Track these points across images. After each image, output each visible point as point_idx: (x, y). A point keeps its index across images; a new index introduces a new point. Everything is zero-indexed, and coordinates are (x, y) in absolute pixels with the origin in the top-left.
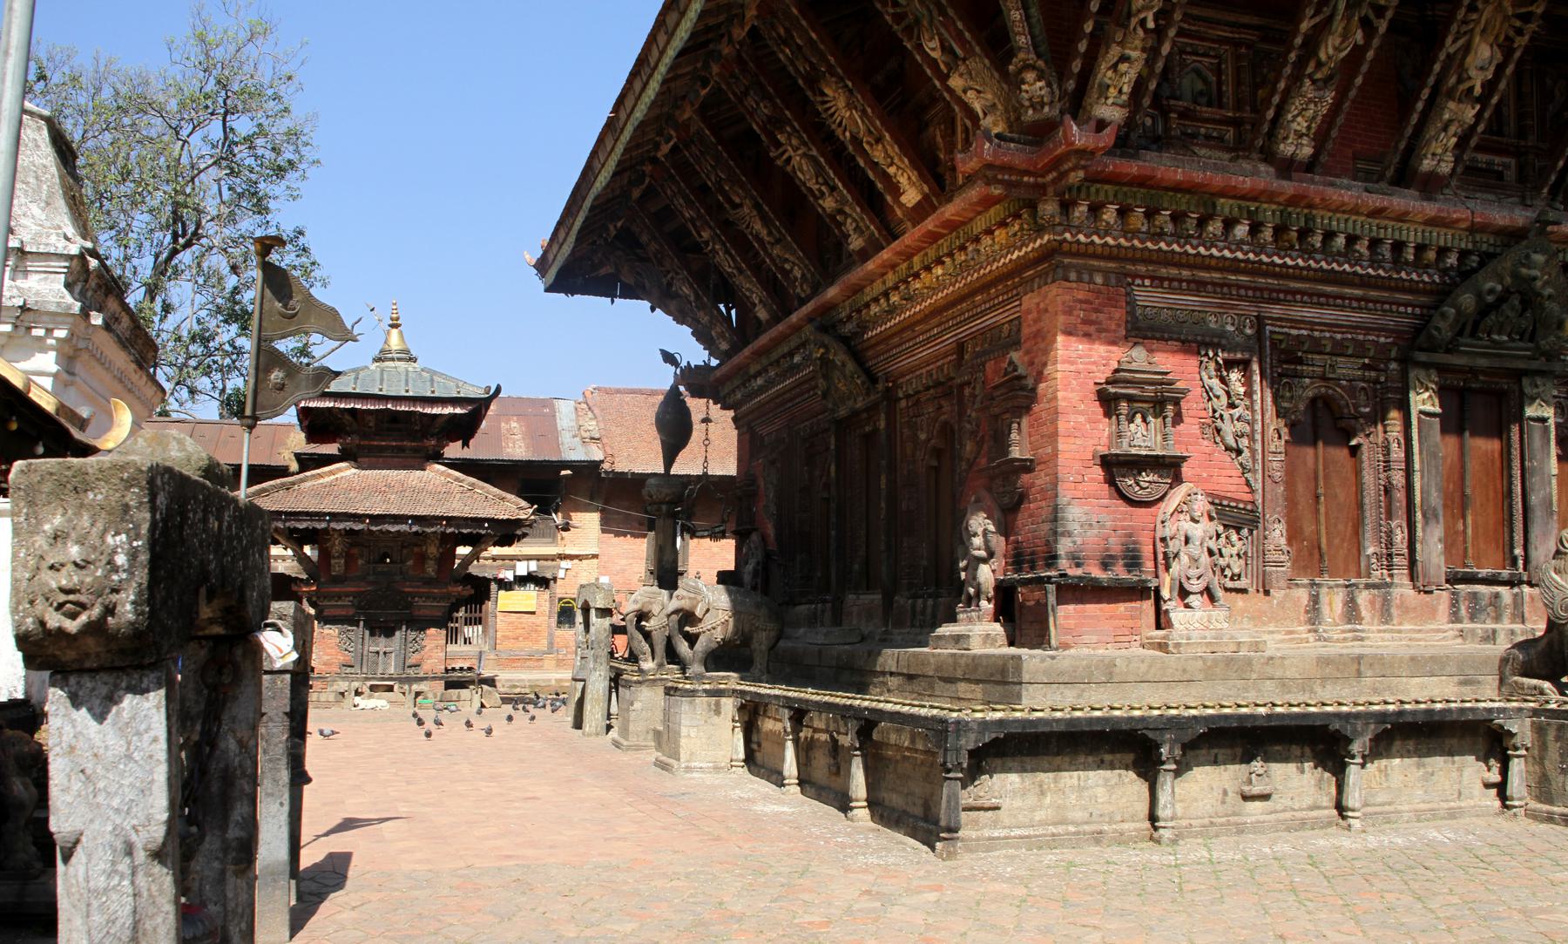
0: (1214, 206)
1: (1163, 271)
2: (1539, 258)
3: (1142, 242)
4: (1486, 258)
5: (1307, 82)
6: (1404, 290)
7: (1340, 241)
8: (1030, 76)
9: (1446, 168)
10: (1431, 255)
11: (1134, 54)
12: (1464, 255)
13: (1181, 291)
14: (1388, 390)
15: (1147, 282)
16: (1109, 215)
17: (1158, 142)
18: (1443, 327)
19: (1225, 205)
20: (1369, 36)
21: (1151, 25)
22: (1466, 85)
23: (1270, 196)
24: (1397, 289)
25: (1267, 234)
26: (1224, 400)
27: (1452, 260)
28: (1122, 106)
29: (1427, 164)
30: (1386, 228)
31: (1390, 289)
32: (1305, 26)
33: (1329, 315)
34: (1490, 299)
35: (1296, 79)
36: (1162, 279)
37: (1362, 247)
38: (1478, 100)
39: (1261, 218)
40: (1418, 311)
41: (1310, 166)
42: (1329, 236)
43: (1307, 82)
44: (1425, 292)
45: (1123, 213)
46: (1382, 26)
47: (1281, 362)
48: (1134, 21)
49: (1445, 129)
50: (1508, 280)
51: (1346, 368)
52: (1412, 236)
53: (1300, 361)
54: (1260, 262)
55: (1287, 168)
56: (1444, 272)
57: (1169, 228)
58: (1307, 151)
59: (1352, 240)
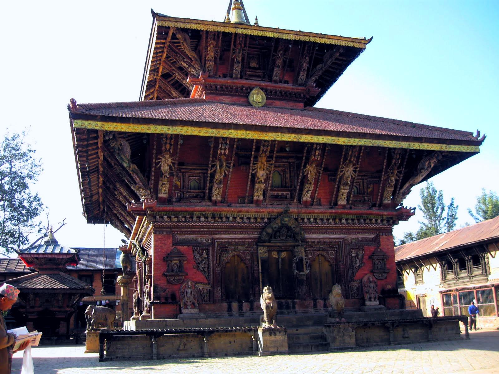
0: (193, 214)
2: (286, 219)
3: (176, 223)
4: (275, 219)
5: (215, 184)
6: (254, 229)
7: (231, 219)
8: (141, 190)
9: (261, 198)
11: (165, 183)
12: (268, 219)
14: (254, 252)
15: (178, 233)
16: (166, 218)
17: (180, 200)
18: (264, 236)
19: (196, 214)
20: (229, 172)
21: (168, 176)
22: (259, 180)
23: (209, 211)
24: (252, 229)
25: (210, 219)
26: (200, 259)
27: (266, 220)
28: (166, 193)
30: (243, 215)
31: (249, 229)
32: (209, 172)
33: (232, 236)
34: (275, 229)
35: (212, 182)
36: (183, 232)
37: (238, 220)
38: (264, 183)
39: (207, 216)
40: (259, 233)
41: (222, 202)
42: (228, 218)
43: (215, 184)
44: (260, 229)
46: (231, 170)
47: (221, 248)
48: (163, 176)
49: (258, 190)
50: (280, 224)
51: (240, 248)
52: (252, 215)
54: (210, 225)
55: (215, 203)
56: (266, 223)
57: (183, 219)
59: (235, 218)
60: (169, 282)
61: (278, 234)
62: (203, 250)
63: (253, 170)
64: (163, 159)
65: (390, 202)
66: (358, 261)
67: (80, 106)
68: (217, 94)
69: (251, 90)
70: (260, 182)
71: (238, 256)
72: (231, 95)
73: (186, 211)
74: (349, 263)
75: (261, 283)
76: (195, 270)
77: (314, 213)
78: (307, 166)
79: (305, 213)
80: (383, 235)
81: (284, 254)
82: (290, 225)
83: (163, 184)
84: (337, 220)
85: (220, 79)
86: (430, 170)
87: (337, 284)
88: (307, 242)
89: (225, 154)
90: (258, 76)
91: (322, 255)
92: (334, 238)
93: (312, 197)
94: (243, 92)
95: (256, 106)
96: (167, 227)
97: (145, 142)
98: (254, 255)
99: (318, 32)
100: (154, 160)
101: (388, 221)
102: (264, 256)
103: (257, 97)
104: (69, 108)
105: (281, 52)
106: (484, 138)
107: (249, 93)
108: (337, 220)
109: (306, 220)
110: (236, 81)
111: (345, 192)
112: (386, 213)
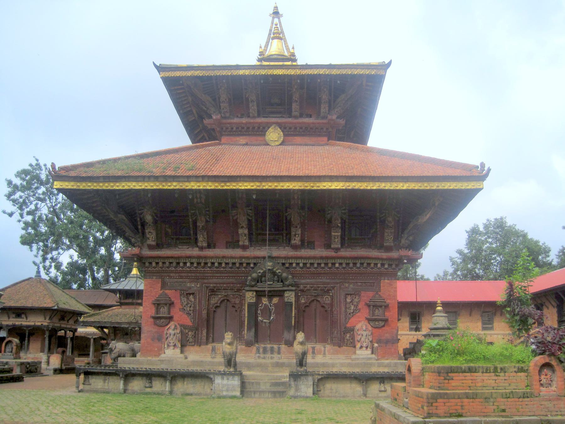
1: (172, 275)
6: (242, 273)
7: (216, 264)
9: (247, 243)
10: (245, 265)
11: (152, 231)
13: (176, 278)
25: (195, 265)
27: (252, 265)
32: (190, 220)
34: (260, 274)
37: (223, 265)
42: (213, 264)
45: (157, 263)
53: (216, 292)
58: (205, 244)
59: (220, 264)
60: (155, 324)
61: (263, 279)
62: (190, 294)
65: (392, 244)
66: (352, 307)
67: (61, 169)
68: (235, 135)
69: (269, 128)
70: (242, 227)
71: (228, 300)
72: (249, 135)
73: (172, 257)
74: (343, 309)
75: (246, 328)
76: (181, 313)
77: (301, 258)
78: (288, 210)
79: (292, 258)
80: (384, 280)
81: (275, 300)
82: (275, 269)
83: (150, 232)
84: (330, 265)
85: (236, 120)
87: (301, 332)
88: (298, 287)
89: (201, 202)
90: (280, 113)
91: (317, 300)
92: (328, 283)
93: (302, 241)
94: (262, 131)
95: (273, 145)
96: (158, 272)
98: (243, 298)
99: (327, 63)
101: (390, 265)
102: (251, 301)
103: (274, 135)
105: (296, 87)
106: (489, 170)
107: (266, 131)
108: (330, 265)
109: (294, 265)
110: (252, 121)
111: (338, 236)
112: (384, 255)
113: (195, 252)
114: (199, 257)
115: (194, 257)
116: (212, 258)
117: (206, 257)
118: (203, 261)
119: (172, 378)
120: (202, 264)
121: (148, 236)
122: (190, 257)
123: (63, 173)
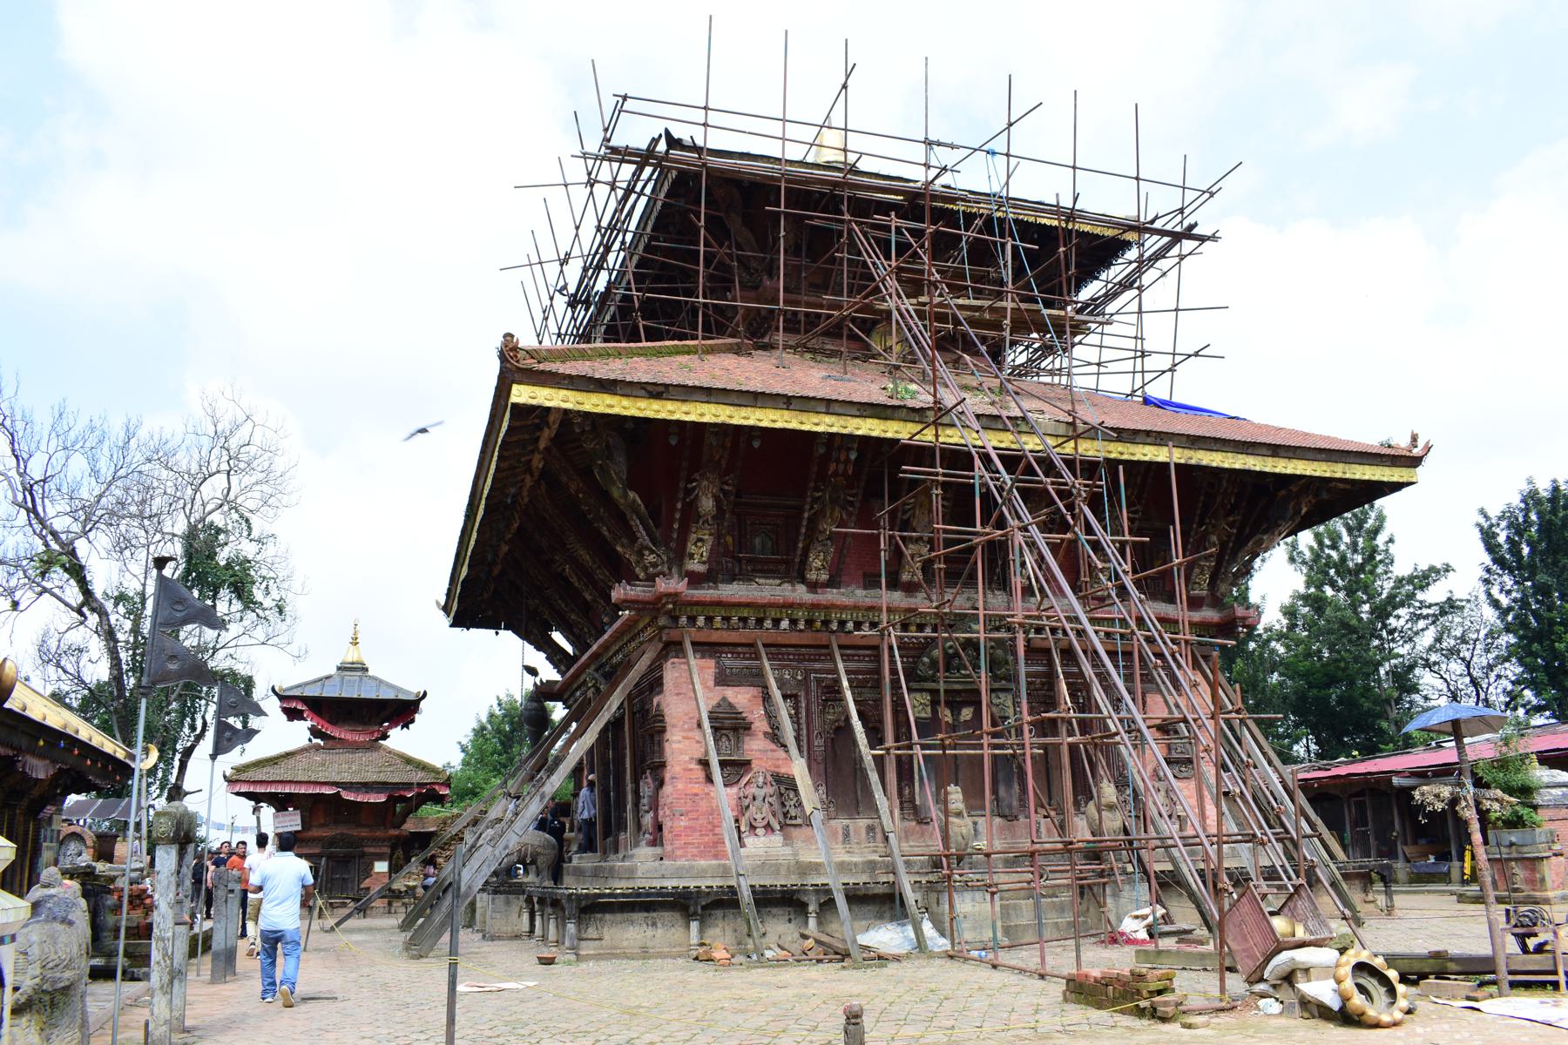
7: (850, 625)
16: (701, 621)
29: (905, 577)
42: (842, 623)
58: (824, 577)
63: (905, 512)
64: (705, 483)
73: (748, 605)
86: (1297, 521)
97: (673, 442)
100: (682, 485)
104: (502, 356)
106: (1428, 449)
113: (800, 593)
114: (815, 606)
115: (801, 605)
116: (843, 608)
117: (829, 607)
118: (820, 616)
119: (821, 905)
120: (818, 624)
121: (691, 548)
122: (791, 606)
123: (530, 363)
